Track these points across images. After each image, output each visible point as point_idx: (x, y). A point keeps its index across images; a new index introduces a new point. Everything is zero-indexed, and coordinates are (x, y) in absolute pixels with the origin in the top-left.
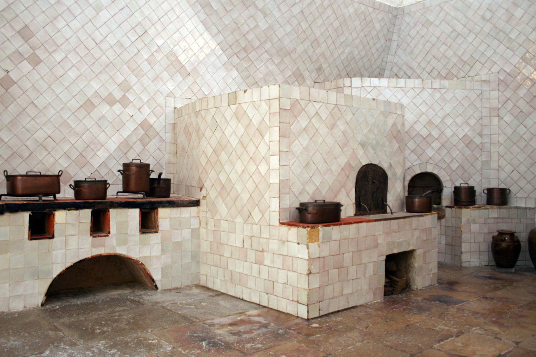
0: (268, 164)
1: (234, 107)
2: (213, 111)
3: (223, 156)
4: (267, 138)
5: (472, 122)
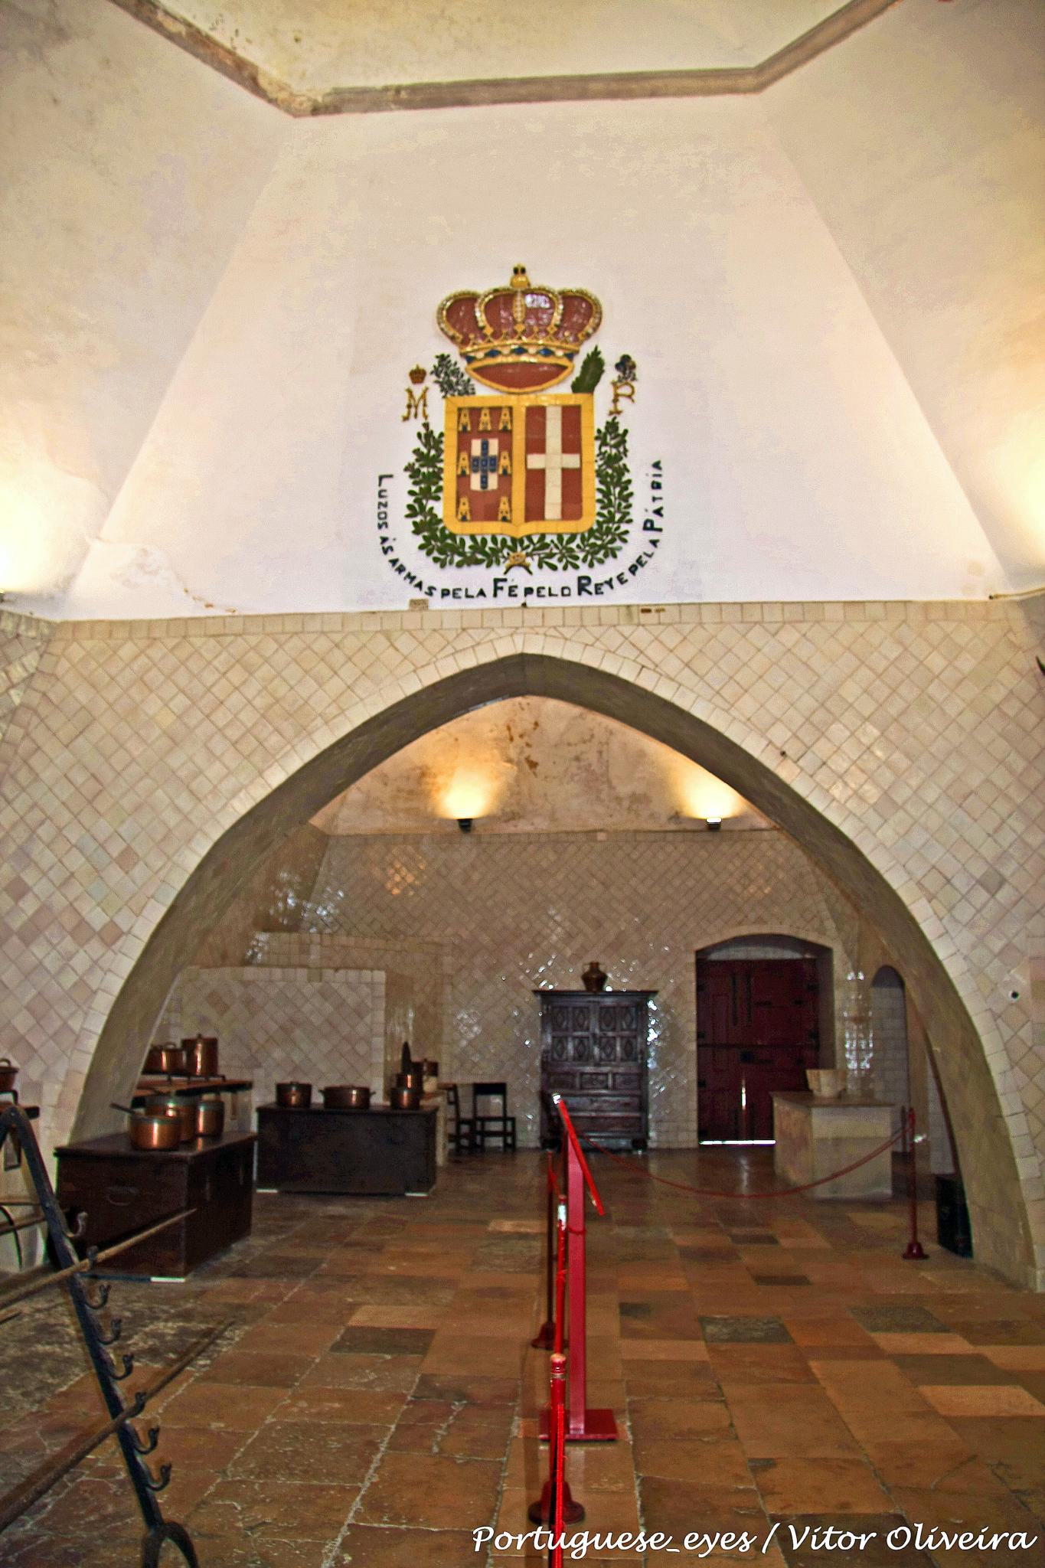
0: (369, 1043)
1: (317, 985)
2: (281, 984)
3: (298, 1033)
4: (368, 1019)
5: (428, 989)
